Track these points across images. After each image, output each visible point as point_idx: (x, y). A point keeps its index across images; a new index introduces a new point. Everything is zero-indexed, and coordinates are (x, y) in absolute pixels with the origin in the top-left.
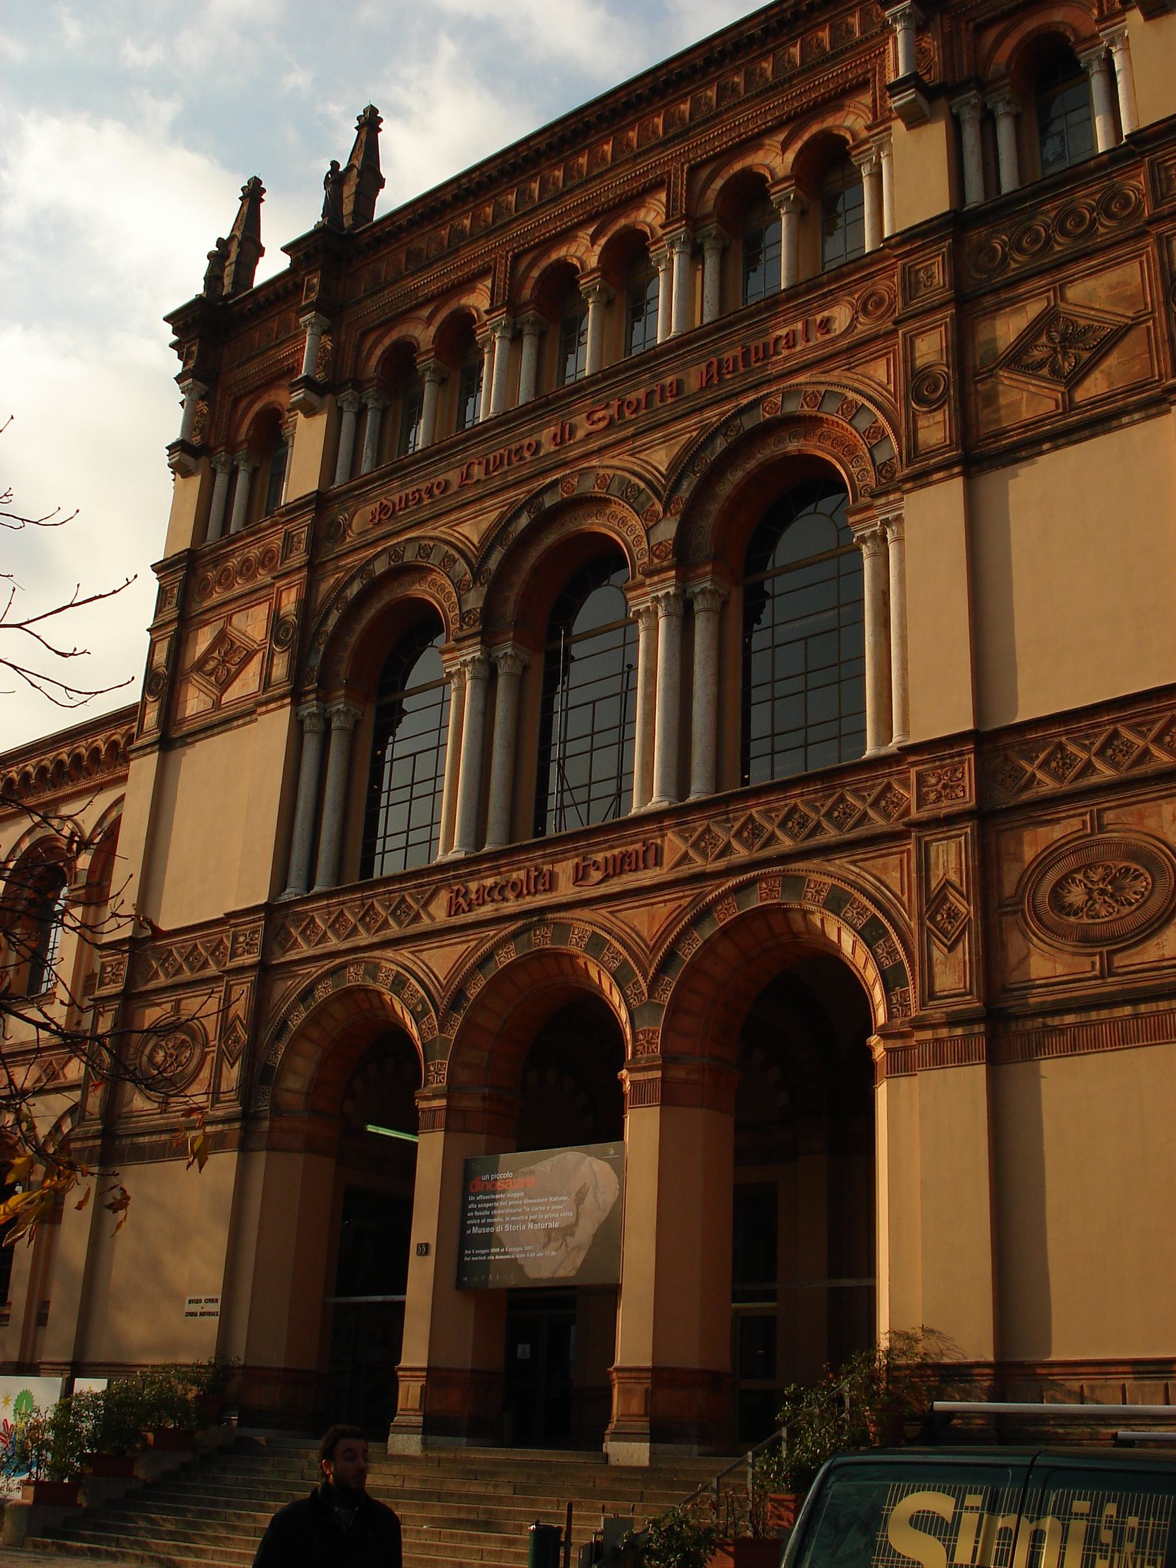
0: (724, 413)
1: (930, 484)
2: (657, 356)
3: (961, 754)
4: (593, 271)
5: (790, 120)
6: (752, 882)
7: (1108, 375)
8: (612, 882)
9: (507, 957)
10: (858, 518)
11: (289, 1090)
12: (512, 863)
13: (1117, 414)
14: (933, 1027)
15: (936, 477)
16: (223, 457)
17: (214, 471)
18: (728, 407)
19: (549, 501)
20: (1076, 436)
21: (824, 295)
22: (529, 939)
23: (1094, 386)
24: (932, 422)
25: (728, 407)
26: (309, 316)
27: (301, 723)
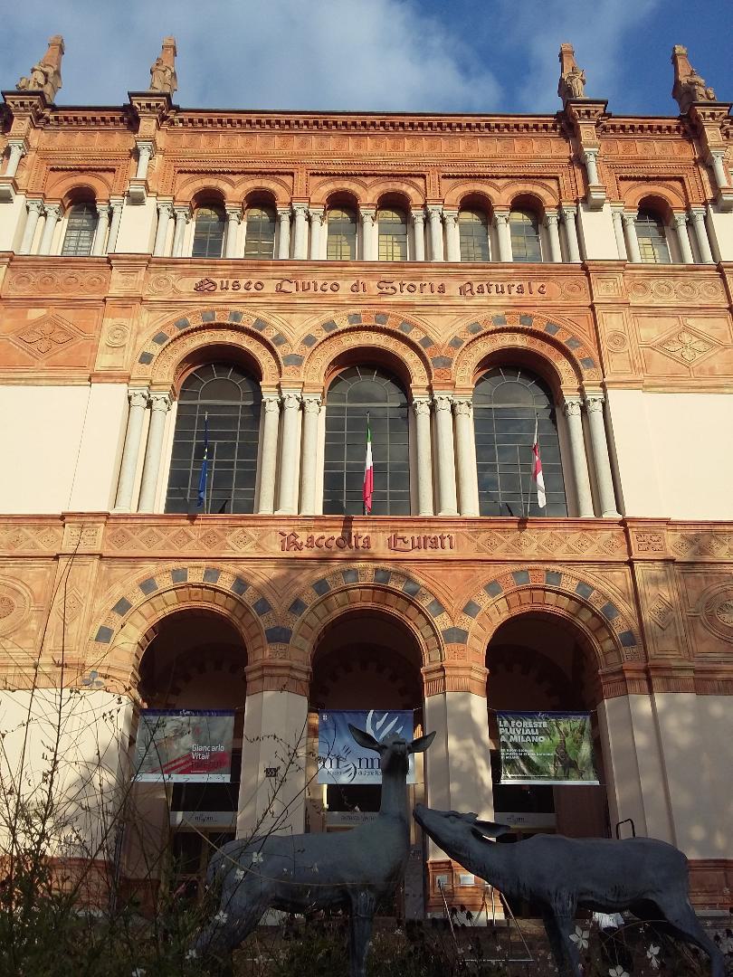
27: (130, 398)
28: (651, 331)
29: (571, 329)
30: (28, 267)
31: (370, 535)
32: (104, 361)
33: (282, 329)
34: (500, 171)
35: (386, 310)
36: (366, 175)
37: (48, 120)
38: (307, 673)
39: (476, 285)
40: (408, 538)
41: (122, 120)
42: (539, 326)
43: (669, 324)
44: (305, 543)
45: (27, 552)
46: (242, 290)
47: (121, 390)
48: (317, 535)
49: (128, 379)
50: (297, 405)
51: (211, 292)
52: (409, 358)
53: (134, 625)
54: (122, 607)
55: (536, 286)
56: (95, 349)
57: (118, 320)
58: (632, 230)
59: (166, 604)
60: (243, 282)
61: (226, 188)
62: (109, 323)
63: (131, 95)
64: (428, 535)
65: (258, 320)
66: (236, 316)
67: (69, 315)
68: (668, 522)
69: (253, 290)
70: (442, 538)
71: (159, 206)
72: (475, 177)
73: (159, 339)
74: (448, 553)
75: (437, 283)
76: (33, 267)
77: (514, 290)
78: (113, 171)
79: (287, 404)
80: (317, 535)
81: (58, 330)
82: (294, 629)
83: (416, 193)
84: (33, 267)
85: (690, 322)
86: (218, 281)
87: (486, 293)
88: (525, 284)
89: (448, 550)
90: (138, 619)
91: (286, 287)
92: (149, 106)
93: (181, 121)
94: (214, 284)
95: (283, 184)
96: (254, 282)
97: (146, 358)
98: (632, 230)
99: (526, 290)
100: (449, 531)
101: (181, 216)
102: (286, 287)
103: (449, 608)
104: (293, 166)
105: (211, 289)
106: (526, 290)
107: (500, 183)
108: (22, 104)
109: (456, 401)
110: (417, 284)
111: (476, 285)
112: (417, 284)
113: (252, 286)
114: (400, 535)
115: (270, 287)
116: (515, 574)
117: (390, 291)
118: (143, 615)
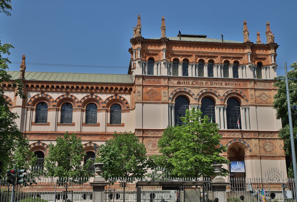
6: (236, 139)
28: (258, 93)
29: (244, 93)
32: (164, 99)
33: (193, 92)
34: (232, 56)
35: (212, 88)
37: (143, 42)
39: (228, 83)
42: (238, 92)
43: (261, 92)
45: (157, 136)
46: (186, 84)
49: (168, 103)
51: (180, 84)
55: (239, 83)
56: (161, 96)
57: (164, 90)
60: (186, 82)
61: (179, 58)
62: (163, 91)
65: (189, 90)
66: (185, 89)
67: (155, 89)
69: (188, 84)
70: (223, 134)
73: (172, 94)
75: (221, 83)
77: (235, 84)
81: (154, 92)
85: (265, 92)
86: (181, 81)
87: (230, 85)
88: (236, 83)
89: (224, 136)
91: (194, 83)
92: (165, 41)
93: (170, 42)
94: (180, 82)
96: (188, 82)
97: (170, 98)
99: (237, 84)
102: (194, 83)
104: (192, 54)
106: (237, 84)
108: (139, 40)
110: (217, 83)
111: (228, 83)
112: (217, 83)
113: (187, 83)
115: (191, 83)
116: (234, 140)
117: (212, 84)
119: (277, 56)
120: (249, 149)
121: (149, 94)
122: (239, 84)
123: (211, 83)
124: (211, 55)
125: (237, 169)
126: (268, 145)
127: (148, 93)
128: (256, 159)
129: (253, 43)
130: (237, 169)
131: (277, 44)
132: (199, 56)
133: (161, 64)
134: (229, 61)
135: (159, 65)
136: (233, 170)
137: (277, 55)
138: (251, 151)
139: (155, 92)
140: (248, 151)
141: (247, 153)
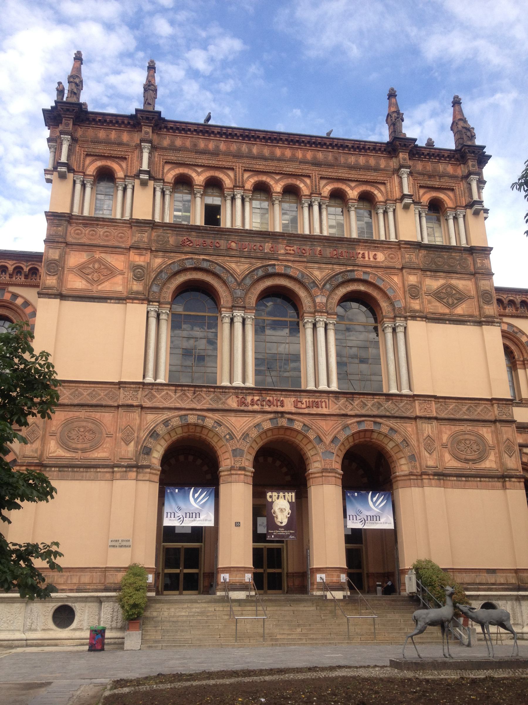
0: (342, 269)
1: (416, 320)
2: (314, 239)
3: (431, 401)
4: (279, 193)
5: (357, 181)
7: (463, 309)
8: (311, 409)
9: (267, 425)
10: (387, 320)
11: (154, 457)
12: (268, 394)
13: (466, 321)
14: (428, 475)
15: (418, 319)
16: (81, 177)
17: (74, 182)
18: (343, 268)
19: (271, 270)
20: (455, 323)
21: (375, 247)
22: (277, 421)
23: (459, 310)
24: (415, 302)
25: (343, 268)
26: (148, 144)
30: (80, 223)
31: (284, 399)
35: (290, 264)
36: (276, 173)
38: (252, 472)
40: (304, 401)
41: (129, 123)
44: (250, 402)
47: (143, 308)
48: (256, 398)
50: (241, 320)
52: (302, 293)
53: (161, 445)
54: (153, 434)
58: (424, 220)
59: (176, 433)
63: (137, 110)
64: (313, 400)
68: (435, 397)
70: (322, 402)
71: (155, 186)
72: (339, 179)
74: (325, 411)
76: (83, 224)
78: (125, 159)
79: (235, 320)
80: (256, 398)
81: (103, 267)
82: (245, 450)
83: (305, 187)
84: (83, 224)
90: (163, 442)
95: (229, 176)
98: (424, 220)
100: (324, 399)
101: (167, 192)
103: (324, 439)
105: (191, 245)
107: (353, 184)
109: (328, 322)
114: (299, 400)
118: (165, 440)
119: (486, 186)
120: (407, 452)
121: (87, 271)
122: (375, 255)
123: (288, 248)
124: (291, 170)
125: (369, 518)
126: (468, 442)
127: (84, 268)
128: (431, 486)
129: (415, 140)
130: (369, 518)
131: (484, 147)
132: (253, 171)
133: (133, 186)
134: (346, 192)
135: (129, 192)
136: (355, 521)
137: (484, 182)
138: (412, 458)
139: (107, 268)
140: (403, 461)
141: (403, 467)
